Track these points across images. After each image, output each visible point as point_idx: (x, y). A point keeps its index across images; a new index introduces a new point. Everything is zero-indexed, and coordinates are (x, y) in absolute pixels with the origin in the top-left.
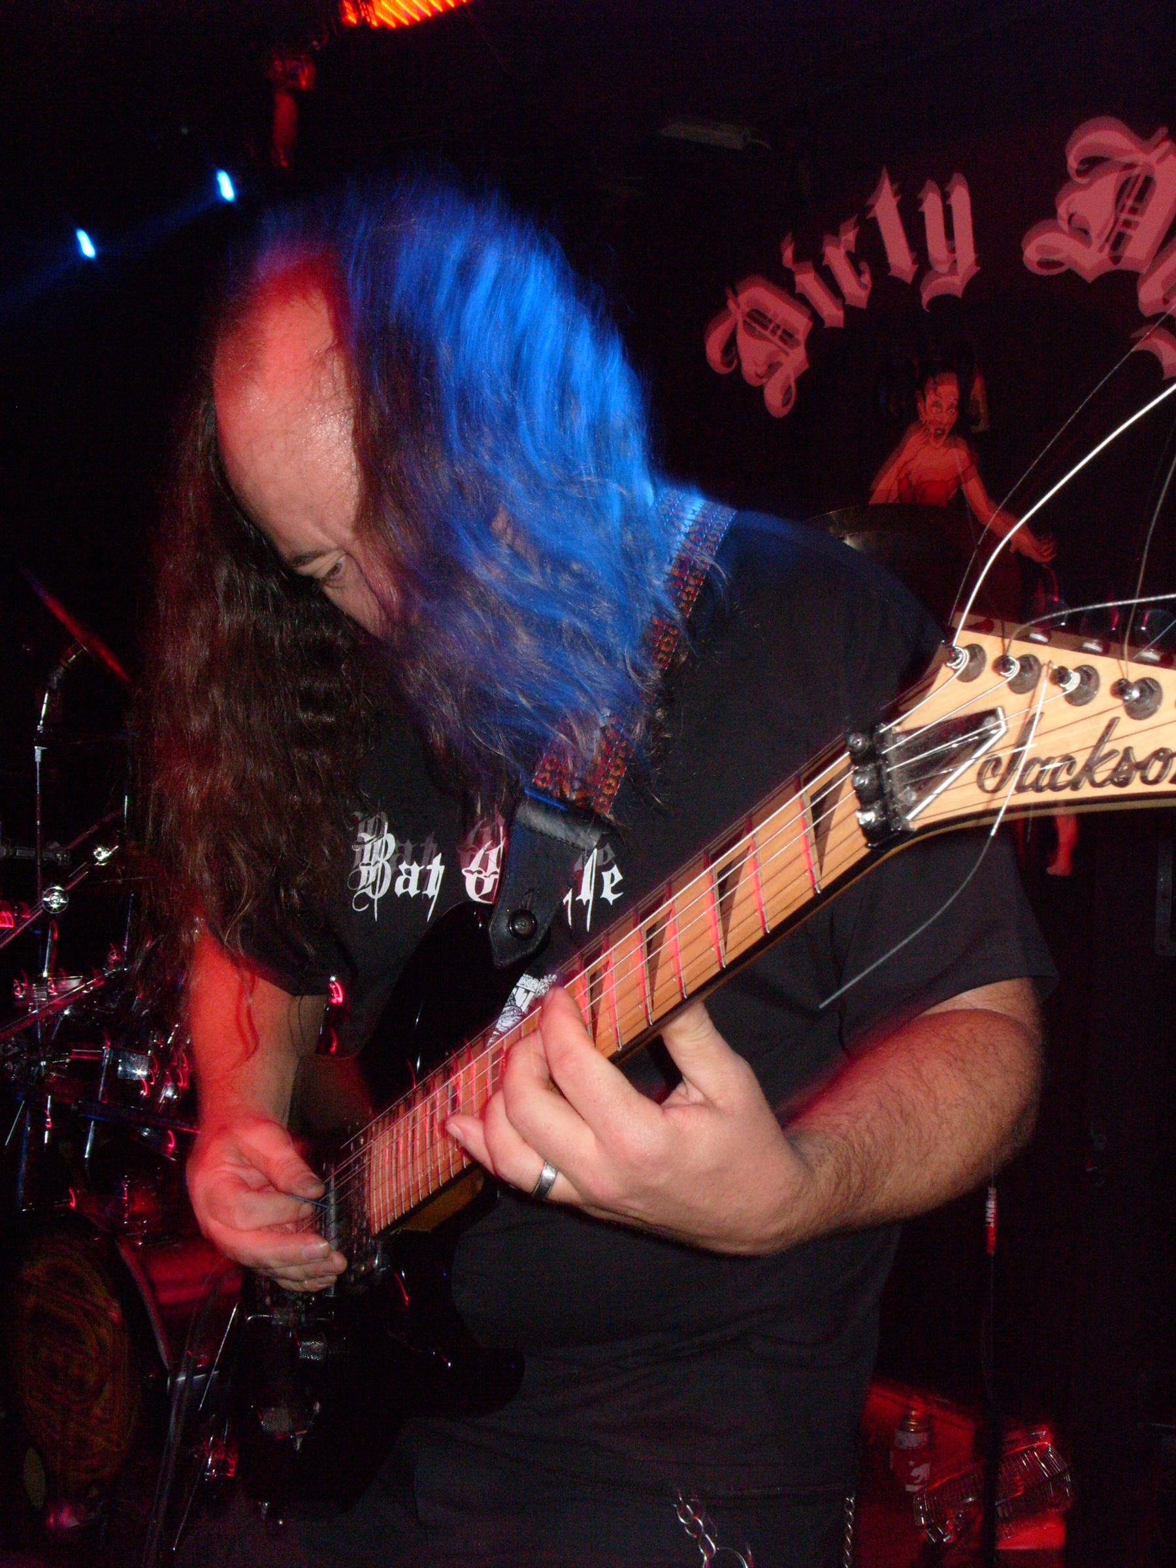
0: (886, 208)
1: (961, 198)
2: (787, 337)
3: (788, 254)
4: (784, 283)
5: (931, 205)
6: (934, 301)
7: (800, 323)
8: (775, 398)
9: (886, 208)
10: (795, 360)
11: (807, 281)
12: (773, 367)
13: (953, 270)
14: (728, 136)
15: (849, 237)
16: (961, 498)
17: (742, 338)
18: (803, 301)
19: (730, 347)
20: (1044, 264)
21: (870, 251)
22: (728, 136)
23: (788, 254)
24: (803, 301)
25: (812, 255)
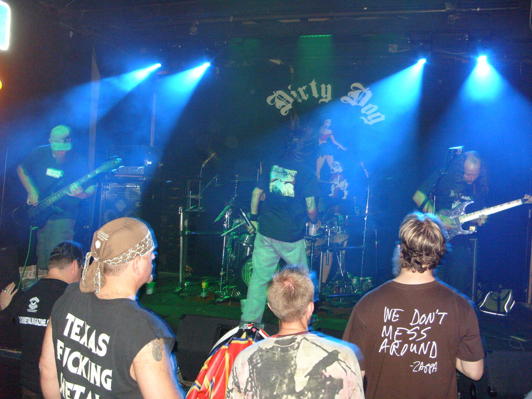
0: (313, 84)
1: (329, 87)
2: (288, 102)
3: (289, 87)
4: (288, 92)
5: (323, 86)
6: (321, 102)
7: (291, 100)
8: (283, 112)
9: (313, 84)
10: (289, 106)
11: (293, 93)
12: (283, 106)
13: (326, 98)
14: (278, 62)
15: (304, 88)
16: (329, 138)
17: (276, 100)
18: (292, 96)
19: (273, 101)
20: (344, 101)
21: (309, 91)
22: (278, 62)
23: (289, 87)
24: (292, 96)
25: (295, 88)
